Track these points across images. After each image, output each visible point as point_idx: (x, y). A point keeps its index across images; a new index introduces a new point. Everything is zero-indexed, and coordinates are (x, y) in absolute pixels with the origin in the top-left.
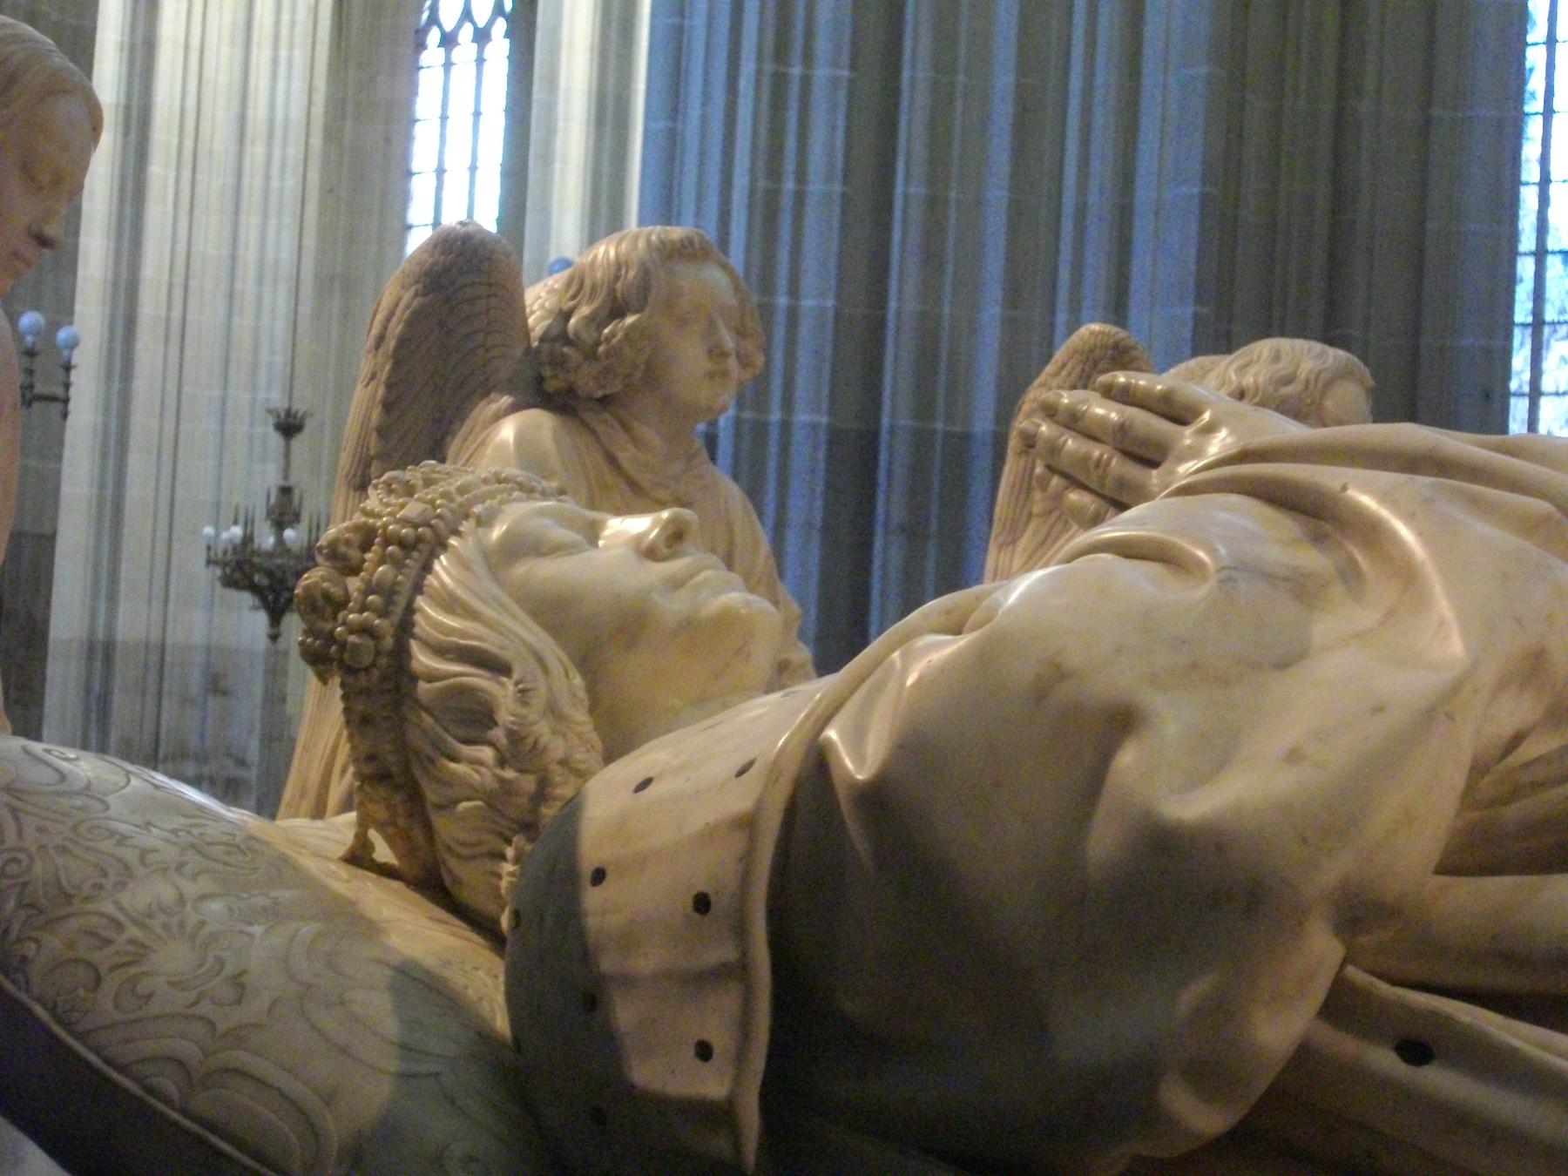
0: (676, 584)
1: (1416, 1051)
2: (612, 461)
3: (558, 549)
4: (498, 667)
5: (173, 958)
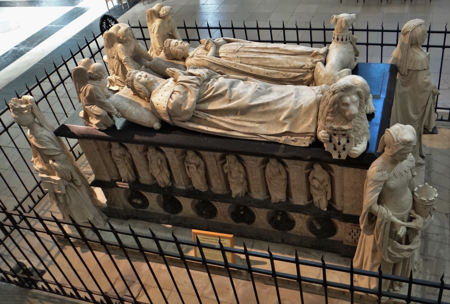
0: (148, 79)
1: (197, 114)
2: (127, 46)
3: (141, 79)
4: (141, 89)
5: (134, 112)
